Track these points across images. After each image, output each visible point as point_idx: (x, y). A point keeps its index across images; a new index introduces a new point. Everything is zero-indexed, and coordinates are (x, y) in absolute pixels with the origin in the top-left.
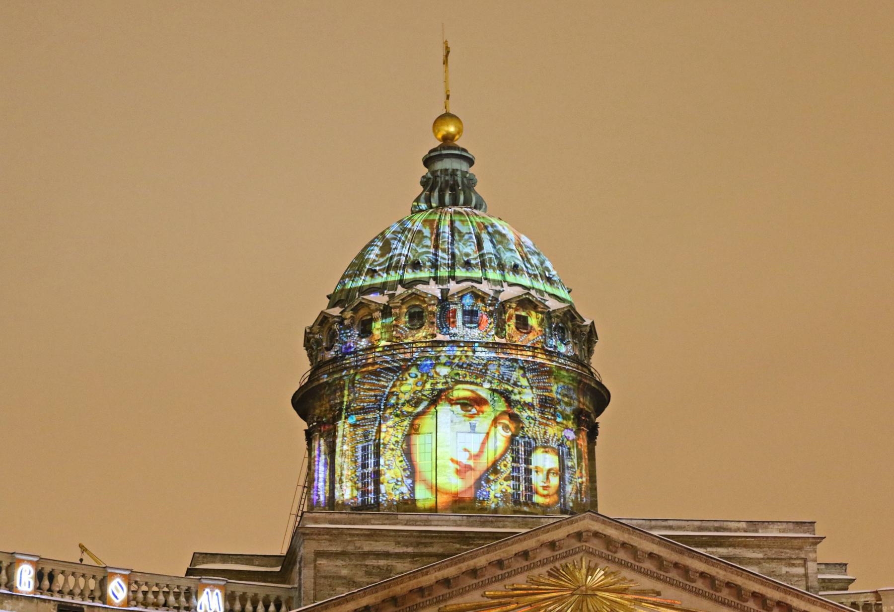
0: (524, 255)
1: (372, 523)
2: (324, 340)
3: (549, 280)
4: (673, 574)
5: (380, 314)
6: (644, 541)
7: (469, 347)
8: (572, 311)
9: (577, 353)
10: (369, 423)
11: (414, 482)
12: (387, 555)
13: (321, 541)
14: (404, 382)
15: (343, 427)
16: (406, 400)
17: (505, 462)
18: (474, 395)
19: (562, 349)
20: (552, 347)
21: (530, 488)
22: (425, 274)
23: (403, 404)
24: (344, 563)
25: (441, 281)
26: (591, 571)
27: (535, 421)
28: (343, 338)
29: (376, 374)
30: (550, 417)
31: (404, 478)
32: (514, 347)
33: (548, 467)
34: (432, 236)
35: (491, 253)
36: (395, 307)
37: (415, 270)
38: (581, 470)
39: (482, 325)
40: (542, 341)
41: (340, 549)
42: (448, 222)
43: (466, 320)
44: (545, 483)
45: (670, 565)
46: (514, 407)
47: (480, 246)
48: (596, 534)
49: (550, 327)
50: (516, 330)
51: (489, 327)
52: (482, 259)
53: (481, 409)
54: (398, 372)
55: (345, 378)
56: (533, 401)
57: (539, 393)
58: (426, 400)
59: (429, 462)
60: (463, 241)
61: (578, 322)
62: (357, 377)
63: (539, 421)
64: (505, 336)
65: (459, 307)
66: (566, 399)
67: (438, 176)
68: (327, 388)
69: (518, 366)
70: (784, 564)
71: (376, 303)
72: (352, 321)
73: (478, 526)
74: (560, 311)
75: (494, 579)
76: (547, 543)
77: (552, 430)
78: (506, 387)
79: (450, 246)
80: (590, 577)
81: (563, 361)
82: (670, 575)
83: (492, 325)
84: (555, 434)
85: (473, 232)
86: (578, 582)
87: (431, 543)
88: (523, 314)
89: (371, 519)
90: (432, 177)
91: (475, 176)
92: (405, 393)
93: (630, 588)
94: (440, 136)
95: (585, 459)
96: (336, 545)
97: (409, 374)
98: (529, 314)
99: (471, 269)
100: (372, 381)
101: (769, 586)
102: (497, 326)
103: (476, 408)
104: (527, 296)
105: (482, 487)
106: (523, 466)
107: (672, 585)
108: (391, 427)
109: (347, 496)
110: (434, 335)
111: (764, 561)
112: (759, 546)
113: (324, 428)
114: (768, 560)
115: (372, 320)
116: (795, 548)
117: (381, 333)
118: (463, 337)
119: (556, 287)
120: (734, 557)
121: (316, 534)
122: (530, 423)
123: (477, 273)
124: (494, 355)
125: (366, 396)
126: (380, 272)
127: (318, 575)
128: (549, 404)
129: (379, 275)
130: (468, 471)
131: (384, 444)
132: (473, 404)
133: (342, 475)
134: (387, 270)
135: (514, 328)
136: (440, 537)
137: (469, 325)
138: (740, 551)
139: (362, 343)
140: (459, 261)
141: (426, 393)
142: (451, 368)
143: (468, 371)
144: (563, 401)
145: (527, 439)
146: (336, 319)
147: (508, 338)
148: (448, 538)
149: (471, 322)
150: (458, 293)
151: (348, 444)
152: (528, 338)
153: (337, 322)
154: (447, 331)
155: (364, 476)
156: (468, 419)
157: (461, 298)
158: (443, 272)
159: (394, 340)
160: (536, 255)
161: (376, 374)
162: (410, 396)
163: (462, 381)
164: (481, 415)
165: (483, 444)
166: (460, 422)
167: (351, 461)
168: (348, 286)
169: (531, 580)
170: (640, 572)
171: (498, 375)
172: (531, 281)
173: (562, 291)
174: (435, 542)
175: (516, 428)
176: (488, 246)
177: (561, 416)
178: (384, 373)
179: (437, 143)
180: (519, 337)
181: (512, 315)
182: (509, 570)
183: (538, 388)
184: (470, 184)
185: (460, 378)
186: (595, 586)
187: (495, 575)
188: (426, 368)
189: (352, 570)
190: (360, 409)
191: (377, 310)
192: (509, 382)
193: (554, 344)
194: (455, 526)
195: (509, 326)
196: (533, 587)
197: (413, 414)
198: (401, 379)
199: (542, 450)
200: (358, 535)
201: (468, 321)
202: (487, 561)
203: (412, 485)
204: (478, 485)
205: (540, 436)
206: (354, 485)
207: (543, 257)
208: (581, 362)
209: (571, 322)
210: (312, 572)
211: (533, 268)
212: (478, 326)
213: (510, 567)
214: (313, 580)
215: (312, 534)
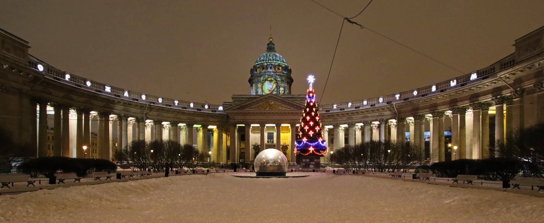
3: (284, 62)
4: (284, 102)
12: (244, 101)
15: (254, 85)
19: (285, 72)
22: (265, 62)
26: (271, 102)
29: (257, 77)
47: (273, 57)
48: (272, 97)
77: (283, 85)
109: (254, 94)
123: (272, 61)
134: (259, 62)
157: (269, 65)
158: (267, 61)
161: (257, 77)
165: (273, 86)
176: (274, 57)
184: (274, 48)
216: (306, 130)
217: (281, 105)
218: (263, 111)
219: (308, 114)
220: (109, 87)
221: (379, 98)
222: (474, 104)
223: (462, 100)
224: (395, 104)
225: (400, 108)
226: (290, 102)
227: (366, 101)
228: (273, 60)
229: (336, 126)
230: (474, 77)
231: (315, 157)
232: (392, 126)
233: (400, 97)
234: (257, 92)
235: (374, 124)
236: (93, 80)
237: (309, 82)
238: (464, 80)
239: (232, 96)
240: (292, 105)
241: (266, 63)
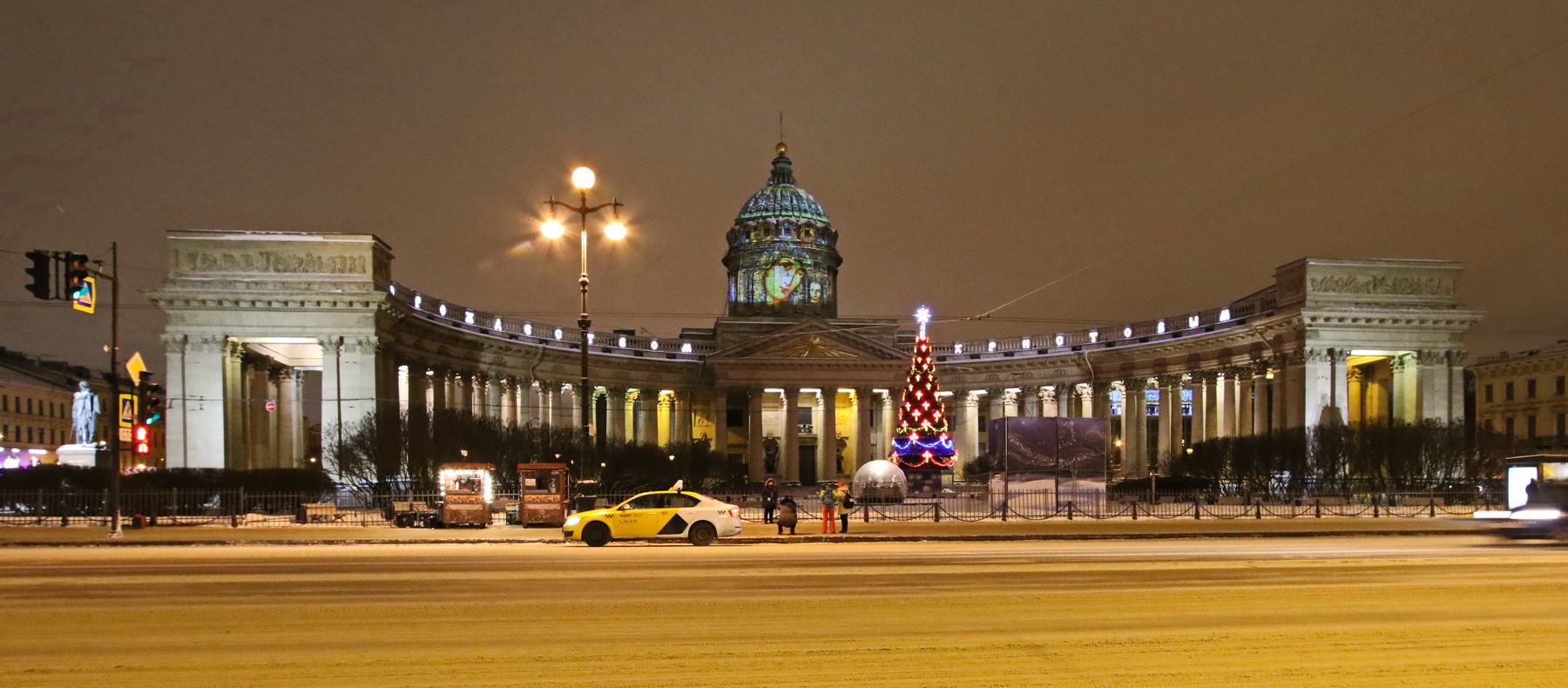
3: (819, 215)
12: (747, 332)
15: (740, 273)
19: (823, 242)
22: (770, 214)
26: (815, 339)
47: (792, 202)
77: (818, 275)
115: (750, 232)
134: (756, 211)
155: (748, 292)
158: (777, 213)
161: (752, 253)
176: (795, 202)
184: (790, 173)
204: (790, 296)
208: (831, 248)
216: (916, 420)
217: (838, 346)
218: (795, 360)
219: (920, 386)
220: (472, 312)
221: (1055, 337)
222: (1225, 368)
223: (1206, 358)
224: (1089, 353)
225: (1097, 361)
226: (859, 340)
227: (1028, 341)
228: (793, 211)
229: (961, 395)
230: (1225, 316)
231: (933, 471)
232: (1084, 396)
233: (1098, 338)
234: (750, 293)
235: (1046, 390)
236: (477, 309)
237: (919, 321)
238: (1209, 322)
240: (866, 348)
241: (775, 216)
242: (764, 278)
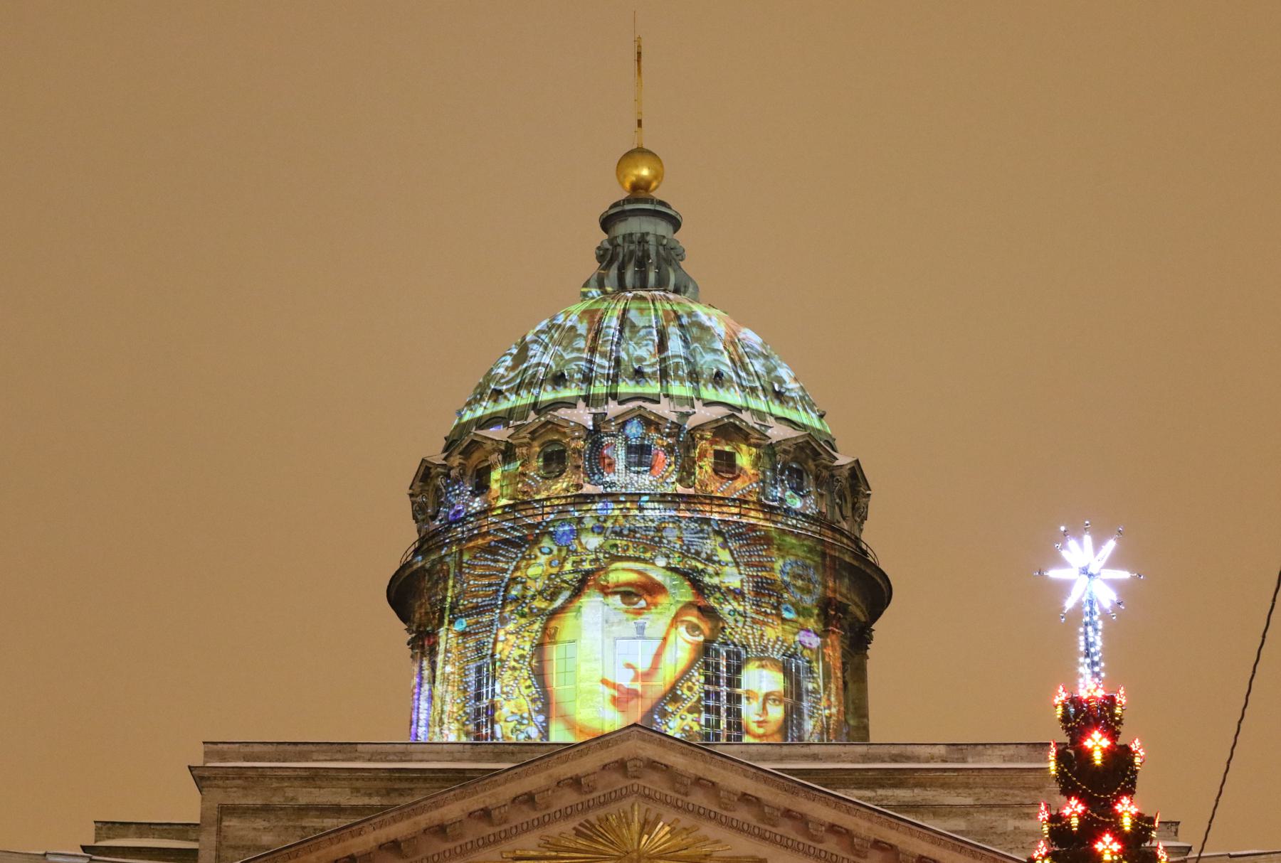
0: (737, 358)
1: (314, 758)
2: (430, 505)
3: (779, 396)
4: (786, 829)
5: (500, 457)
6: (730, 774)
7: (632, 502)
8: (813, 443)
9: (824, 510)
10: (484, 629)
11: (547, 720)
12: (338, 810)
13: (229, 789)
14: (533, 561)
15: (447, 638)
16: (537, 591)
17: (690, 684)
18: (643, 579)
19: (797, 504)
20: (776, 501)
21: (737, 726)
23: (533, 597)
24: (266, 824)
25: (595, 402)
26: (647, 826)
27: (746, 617)
28: (450, 498)
30: (769, 611)
31: (533, 714)
32: (708, 501)
33: (764, 691)
34: (589, 333)
35: (680, 356)
36: (521, 445)
37: (556, 387)
38: (829, 695)
39: (657, 468)
40: (757, 490)
41: (259, 802)
42: (617, 313)
43: (631, 460)
44: (760, 716)
45: (775, 814)
46: (709, 597)
47: (662, 346)
48: (653, 765)
49: (774, 469)
50: (713, 473)
51: (667, 471)
52: (663, 365)
53: (654, 601)
54: (523, 546)
55: (448, 559)
56: (742, 586)
57: (750, 573)
58: (568, 589)
59: (571, 687)
60: (635, 340)
61: (823, 461)
62: (466, 558)
63: (752, 618)
64: (694, 483)
65: (620, 441)
66: (800, 583)
67: (619, 245)
68: (427, 578)
69: (710, 529)
70: (1010, 814)
71: (493, 440)
72: (461, 471)
73: (488, 761)
74: (790, 443)
75: (481, 842)
76: (567, 779)
77: (772, 633)
78: (694, 563)
79: (614, 348)
80: (646, 837)
81: (794, 522)
82: (780, 830)
83: (673, 467)
84: (778, 638)
85: (654, 326)
86: (625, 845)
87: (411, 789)
88: (727, 449)
89: (313, 752)
90: (610, 247)
91: (678, 242)
92: (535, 579)
93: (715, 854)
94: (628, 185)
95: (837, 678)
96: (253, 795)
97: (540, 549)
98: (738, 450)
99: (644, 380)
100: (486, 563)
101: (945, 846)
102: (682, 468)
103: (645, 600)
104: (732, 420)
105: (655, 725)
106: (724, 690)
107: (787, 847)
108: (512, 633)
110: (579, 486)
111: (976, 810)
112: (967, 786)
113: (429, 641)
114: (983, 809)
115: (488, 469)
116: (1029, 787)
117: (502, 486)
118: (626, 487)
119: (792, 407)
120: (924, 803)
121: (222, 778)
122: (736, 621)
123: (653, 388)
124: (673, 513)
125: (478, 585)
126: (507, 394)
127: (224, 843)
128: (768, 590)
129: (506, 397)
130: (633, 698)
131: (501, 660)
132: (641, 592)
133: (443, 712)
135: (710, 470)
136: (425, 780)
137: (636, 468)
138: (934, 793)
139: (476, 505)
140: (625, 370)
141: (568, 577)
142: (605, 537)
143: (631, 541)
144: (794, 585)
145: (732, 647)
146: (439, 469)
147: (699, 488)
148: (437, 780)
149: (640, 464)
150: (616, 418)
151: (454, 664)
152: (733, 486)
153: (442, 473)
154: (600, 478)
155: (478, 712)
156: (631, 616)
157: (624, 425)
158: (600, 388)
159: (520, 497)
160: (761, 358)
161: (491, 550)
162: (544, 583)
163: (621, 557)
164: (653, 610)
165: (658, 655)
166: (620, 622)
167: (459, 690)
168: (465, 419)
169: (548, 844)
170: (732, 827)
171: (681, 546)
172: (745, 397)
173: (803, 414)
174: (416, 788)
175: (712, 630)
176: (675, 345)
177: (793, 611)
178: (503, 549)
179: (625, 195)
180: (718, 484)
181: (706, 450)
182: (506, 826)
183: (748, 565)
184: (671, 256)
185: (618, 552)
186: (653, 852)
187: (484, 835)
188: (565, 538)
189: (279, 836)
190: (473, 608)
191: (494, 451)
192: (699, 557)
193: (779, 495)
194: (451, 761)
195: (701, 467)
196: (548, 854)
197: (547, 612)
198: (527, 557)
199: (757, 663)
200: (289, 778)
201: (635, 462)
202: (463, 811)
203: (544, 724)
205: (755, 641)
206: (461, 727)
207: (776, 360)
209: (814, 460)
210: (213, 839)
211: (751, 378)
212: (650, 470)
213: (505, 822)
214: (214, 853)
215: (215, 778)
226: (863, 827)
228: (664, 375)
234: (483, 714)
239: (199, 762)
242: (540, 648)
